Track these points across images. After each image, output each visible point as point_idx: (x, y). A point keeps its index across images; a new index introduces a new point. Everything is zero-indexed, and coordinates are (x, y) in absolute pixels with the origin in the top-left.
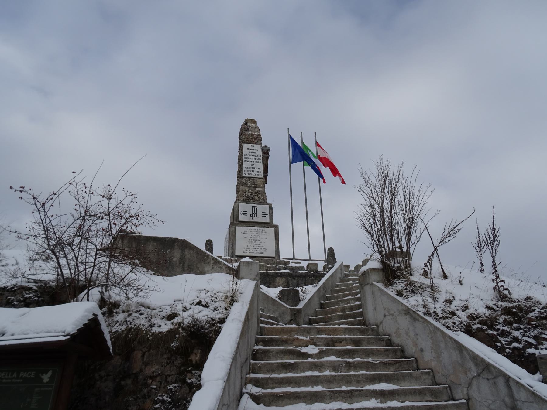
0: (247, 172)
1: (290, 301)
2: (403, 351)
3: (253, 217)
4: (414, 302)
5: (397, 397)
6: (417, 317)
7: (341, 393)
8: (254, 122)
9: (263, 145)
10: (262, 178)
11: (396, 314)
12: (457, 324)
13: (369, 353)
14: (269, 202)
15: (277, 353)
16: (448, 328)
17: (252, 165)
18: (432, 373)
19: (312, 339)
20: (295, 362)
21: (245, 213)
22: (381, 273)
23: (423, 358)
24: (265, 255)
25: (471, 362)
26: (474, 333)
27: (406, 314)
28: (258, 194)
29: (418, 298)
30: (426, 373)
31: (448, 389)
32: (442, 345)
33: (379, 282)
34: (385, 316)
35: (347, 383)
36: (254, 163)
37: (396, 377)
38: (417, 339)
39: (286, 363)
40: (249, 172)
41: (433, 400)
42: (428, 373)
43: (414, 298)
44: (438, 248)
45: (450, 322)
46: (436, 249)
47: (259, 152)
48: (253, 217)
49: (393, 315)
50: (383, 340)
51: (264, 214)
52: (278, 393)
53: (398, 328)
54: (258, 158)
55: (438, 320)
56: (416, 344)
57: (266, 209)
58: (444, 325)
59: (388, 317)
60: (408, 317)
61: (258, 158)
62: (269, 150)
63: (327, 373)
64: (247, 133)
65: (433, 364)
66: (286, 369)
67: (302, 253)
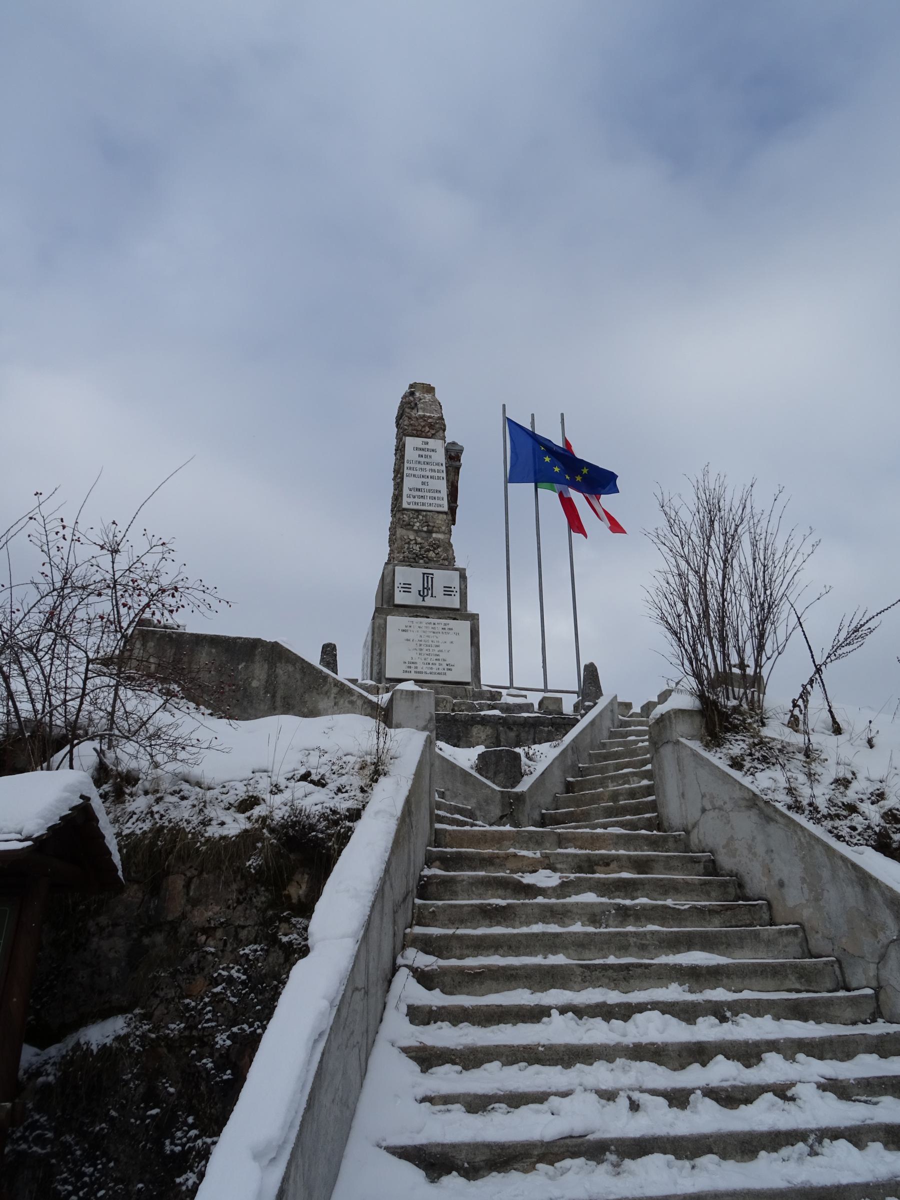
0: (411, 500)
1: (501, 777)
2: (741, 885)
3: (424, 597)
4: (767, 781)
5: (725, 981)
6: (773, 815)
7: (606, 970)
8: (430, 389)
9: (448, 440)
11: (728, 807)
12: (860, 830)
13: (667, 888)
14: (459, 564)
15: (472, 884)
16: (839, 837)
17: (423, 483)
18: (802, 931)
19: (546, 856)
20: (508, 905)
22: (698, 720)
23: (784, 900)
24: (449, 677)
25: (888, 911)
26: (896, 849)
27: (749, 808)
28: (435, 546)
29: (776, 773)
30: (789, 932)
31: (836, 966)
32: (826, 874)
33: (692, 738)
34: (704, 810)
35: (620, 950)
36: (429, 480)
37: (724, 940)
38: (772, 860)
39: (490, 905)
40: (417, 500)
41: (803, 988)
42: (794, 932)
43: (768, 773)
44: (823, 668)
45: (843, 826)
46: (818, 670)
47: (440, 457)
48: (424, 597)
49: (720, 809)
50: (699, 862)
51: (448, 591)
52: (471, 968)
53: (732, 838)
54: (436, 468)
55: (818, 821)
56: (768, 872)
57: (452, 578)
58: (830, 832)
59: (711, 814)
60: (753, 814)
61: (436, 468)
62: (461, 451)
63: (577, 928)
64: (413, 413)
65: (806, 913)
66: (491, 918)
67: (528, 675)
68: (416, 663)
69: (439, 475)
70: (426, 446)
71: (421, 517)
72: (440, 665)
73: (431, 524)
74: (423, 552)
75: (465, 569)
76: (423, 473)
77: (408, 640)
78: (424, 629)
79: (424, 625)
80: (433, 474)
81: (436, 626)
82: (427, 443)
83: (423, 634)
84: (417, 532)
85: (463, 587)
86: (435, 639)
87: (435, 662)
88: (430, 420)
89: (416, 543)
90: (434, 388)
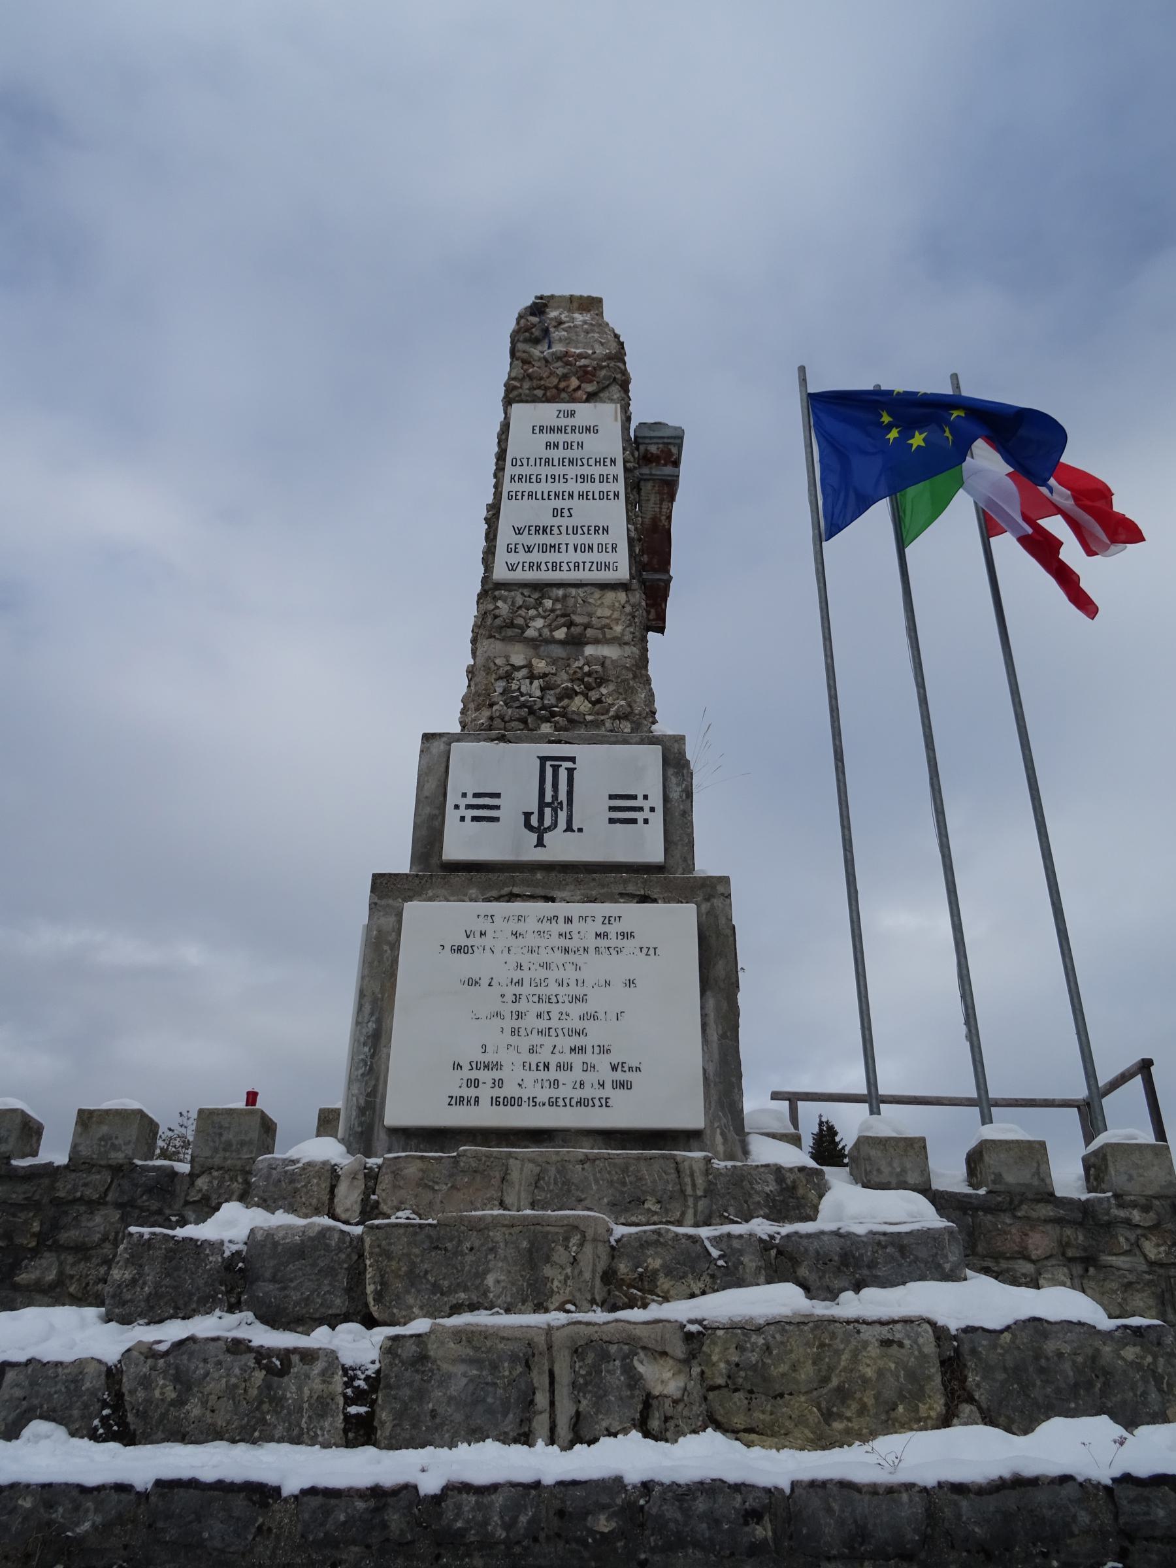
3: (540, 832)
8: (592, 304)
9: (639, 415)
10: (624, 586)
14: (664, 726)
17: (556, 513)
21: (485, 807)
24: (624, 1113)
36: (575, 503)
40: (536, 556)
48: (540, 832)
51: (623, 809)
54: (597, 471)
57: (641, 768)
61: (597, 471)
62: (677, 439)
64: (536, 352)
67: (919, 1055)
68: (498, 1066)
69: (605, 487)
70: (570, 422)
71: (548, 603)
72: (588, 1067)
73: (577, 619)
74: (550, 699)
75: (681, 739)
76: (559, 487)
77: (472, 982)
78: (531, 940)
79: (531, 925)
80: (587, 487)
81: (575, 926)
82: (572, 414)
83: (524, 959)
84: (536, 644)
85: (675, 794)
86: (570, 974)
87: (568, 1057)
88: (583, 362)
89: (532, 677)
90: (600, 301)
